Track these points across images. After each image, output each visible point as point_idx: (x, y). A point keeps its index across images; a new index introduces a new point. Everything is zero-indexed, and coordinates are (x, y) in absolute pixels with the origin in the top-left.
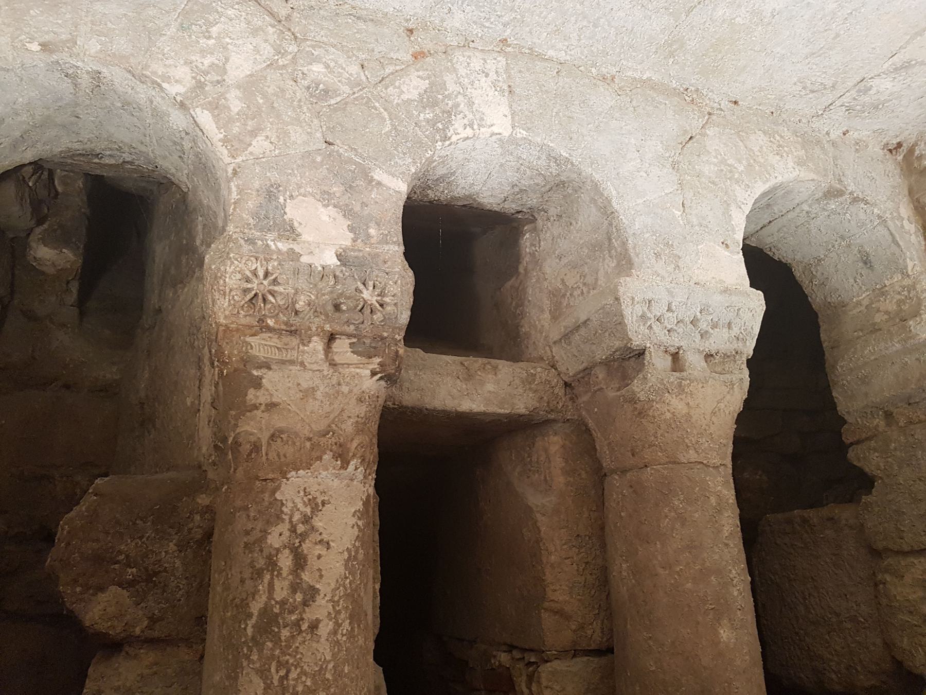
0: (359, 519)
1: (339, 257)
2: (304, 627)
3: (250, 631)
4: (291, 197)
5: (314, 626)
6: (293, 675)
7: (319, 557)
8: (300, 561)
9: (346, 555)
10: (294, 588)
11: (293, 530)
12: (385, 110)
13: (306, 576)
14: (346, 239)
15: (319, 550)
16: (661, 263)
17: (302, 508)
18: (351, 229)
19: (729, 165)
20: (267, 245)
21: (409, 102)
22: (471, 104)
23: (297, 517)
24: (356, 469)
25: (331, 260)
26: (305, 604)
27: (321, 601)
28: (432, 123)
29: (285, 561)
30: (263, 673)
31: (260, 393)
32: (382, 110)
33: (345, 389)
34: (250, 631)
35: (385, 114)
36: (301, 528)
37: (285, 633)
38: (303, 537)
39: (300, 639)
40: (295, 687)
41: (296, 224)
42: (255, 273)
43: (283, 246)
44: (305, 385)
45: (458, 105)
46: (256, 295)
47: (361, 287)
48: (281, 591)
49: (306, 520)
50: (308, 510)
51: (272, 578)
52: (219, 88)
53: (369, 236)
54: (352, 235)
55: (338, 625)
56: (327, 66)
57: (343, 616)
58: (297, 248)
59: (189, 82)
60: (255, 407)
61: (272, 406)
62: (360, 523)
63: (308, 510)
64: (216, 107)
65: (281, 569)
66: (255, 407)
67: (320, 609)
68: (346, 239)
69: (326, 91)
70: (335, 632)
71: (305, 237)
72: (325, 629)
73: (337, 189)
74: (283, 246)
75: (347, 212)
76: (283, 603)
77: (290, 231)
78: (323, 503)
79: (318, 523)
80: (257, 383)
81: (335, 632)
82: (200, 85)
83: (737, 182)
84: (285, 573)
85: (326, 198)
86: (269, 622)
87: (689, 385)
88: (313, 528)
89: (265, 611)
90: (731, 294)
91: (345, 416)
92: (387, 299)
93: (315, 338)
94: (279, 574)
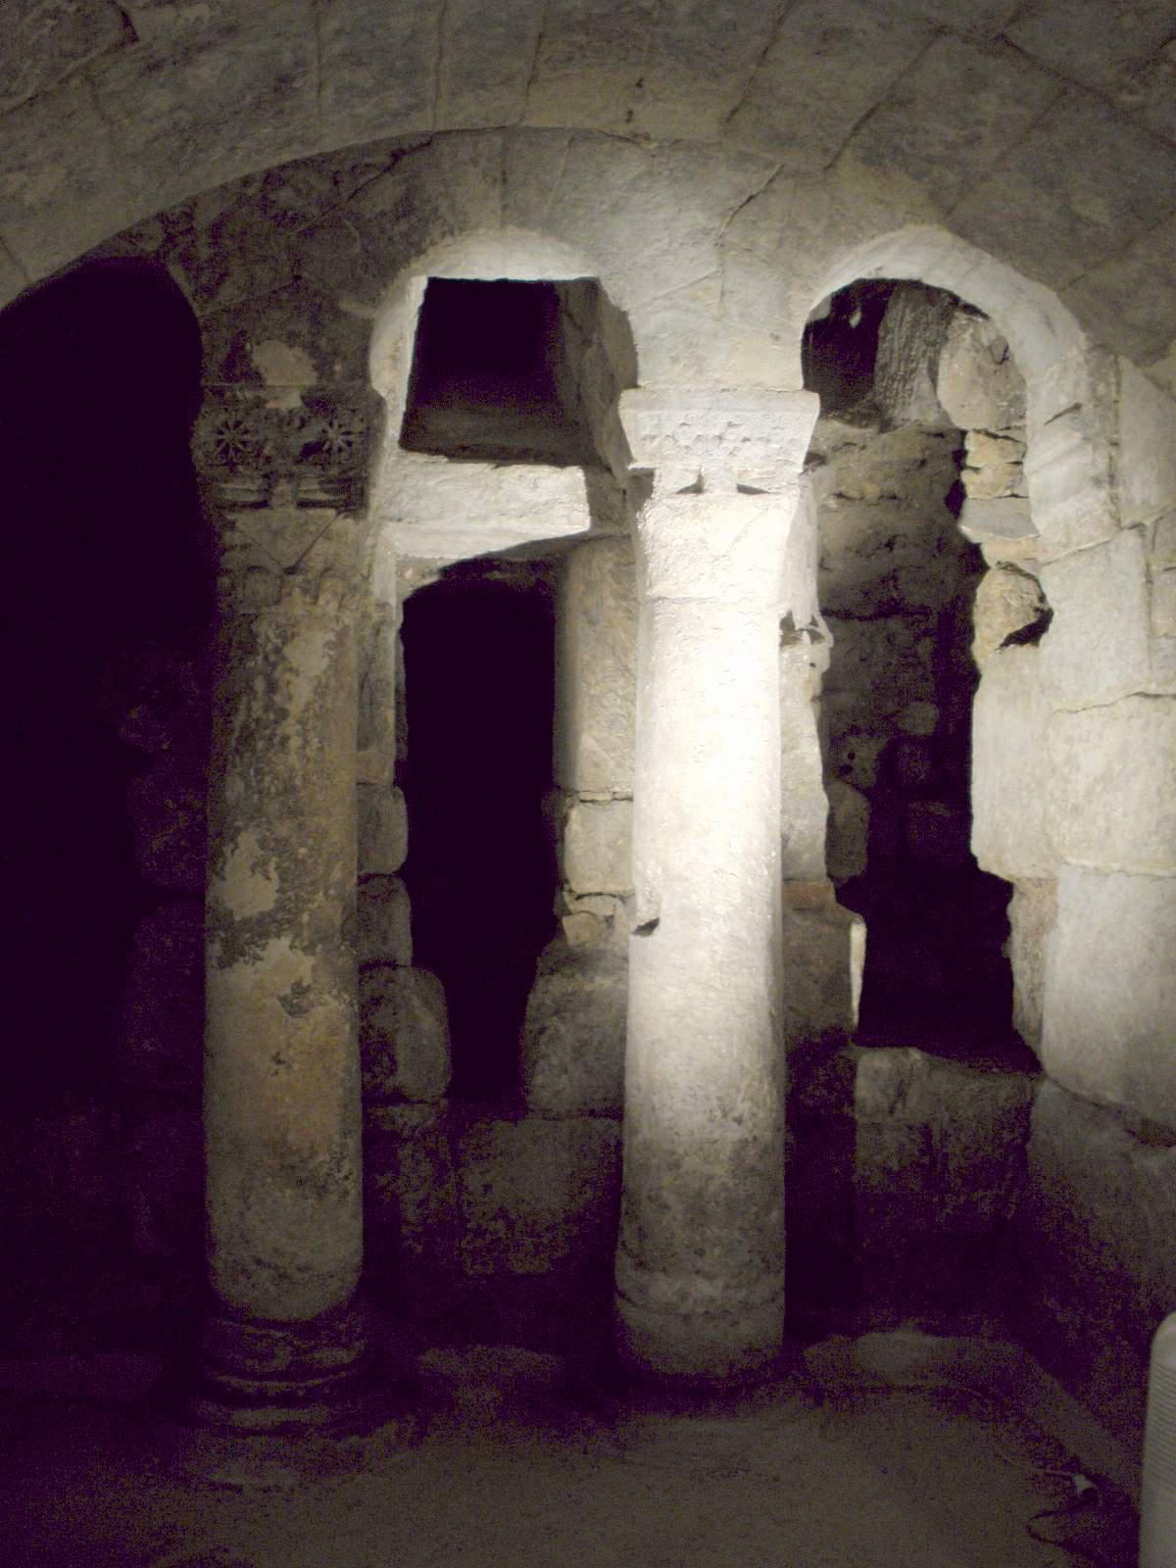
0: (330, 649)
1: (303, 398)
2: (276, 740)
3: (233, 743)
4: (259, 344)
5: (285, 740)
6: (268, 778)
7: (289, 683)
8: (272, 687)
9: (315, 683)
10: (266, 709)
11: (266, 658)
12: (357, 228)
13: (277, 698)
14: (309, 379)
15: (288, 676)
16: (678, 368)
17: (275, 640)
18: (316, 368)
19: (801, 229)
20: (235, 396)
21: (383, 214)
22: (452, 207)
23: (270, 647)
24: (328, 603)
25: (293, 401)
26: (276, 722)
27: (291, 720)
28: (405, 235)
29: (260, 685)
30: (243, 776)
31: (236, 535)
32: (353, 229)
33: (312, 528)
34: (233, 743)
35: (357, 234)
36: (272, 658)
37: (260, 745)
38: (274, 666)
39: (273, 751)
40: (269, 788)
41: (262, 371)
42: (226, 425)
43: (249, 395)
44: (274, 526)
45: (436, 210)
46: (228, 445)
47: (327, 428)
48: (257, 707)
49: (278, 650)
50: (278, 642)
51: (249, 702)
52: (189, 238)
53: (333, 373)
54: (315, 374)
55: (306, 742)
56: (298, 191)
57: (312, 733)
58: (262, 394)
59: (160, 236)
60: (232, 547)
61: (244, 547)
62: (332, 653)
63: (280, 641)
64: (186, 260)
65: (257, 692)
66: (232, 547)
67: (290, 727)
68: (309, 379)
69: (293, 220)
70: (303, 747)
71: (270, 382)
72: (295, 743)
73: (303, 327)
74: (249, 395)
75: (313, 349)
76: (257, 721)
77: (255, 378)
78: (293, 636)
79: (287, 651)
80: (232, 526)
81: (303, 747)
82: (170, 238)
83: (808, 251)
84: (259, 695)
85: (291, 339)
86: (247, 737)
87: (706, 508)
88: (284, 659)
89: (245, 727)
90: (769, 400)
91: (313, 553)
92: (352, 438)
93: (283, 481)
94: (255, 698)
